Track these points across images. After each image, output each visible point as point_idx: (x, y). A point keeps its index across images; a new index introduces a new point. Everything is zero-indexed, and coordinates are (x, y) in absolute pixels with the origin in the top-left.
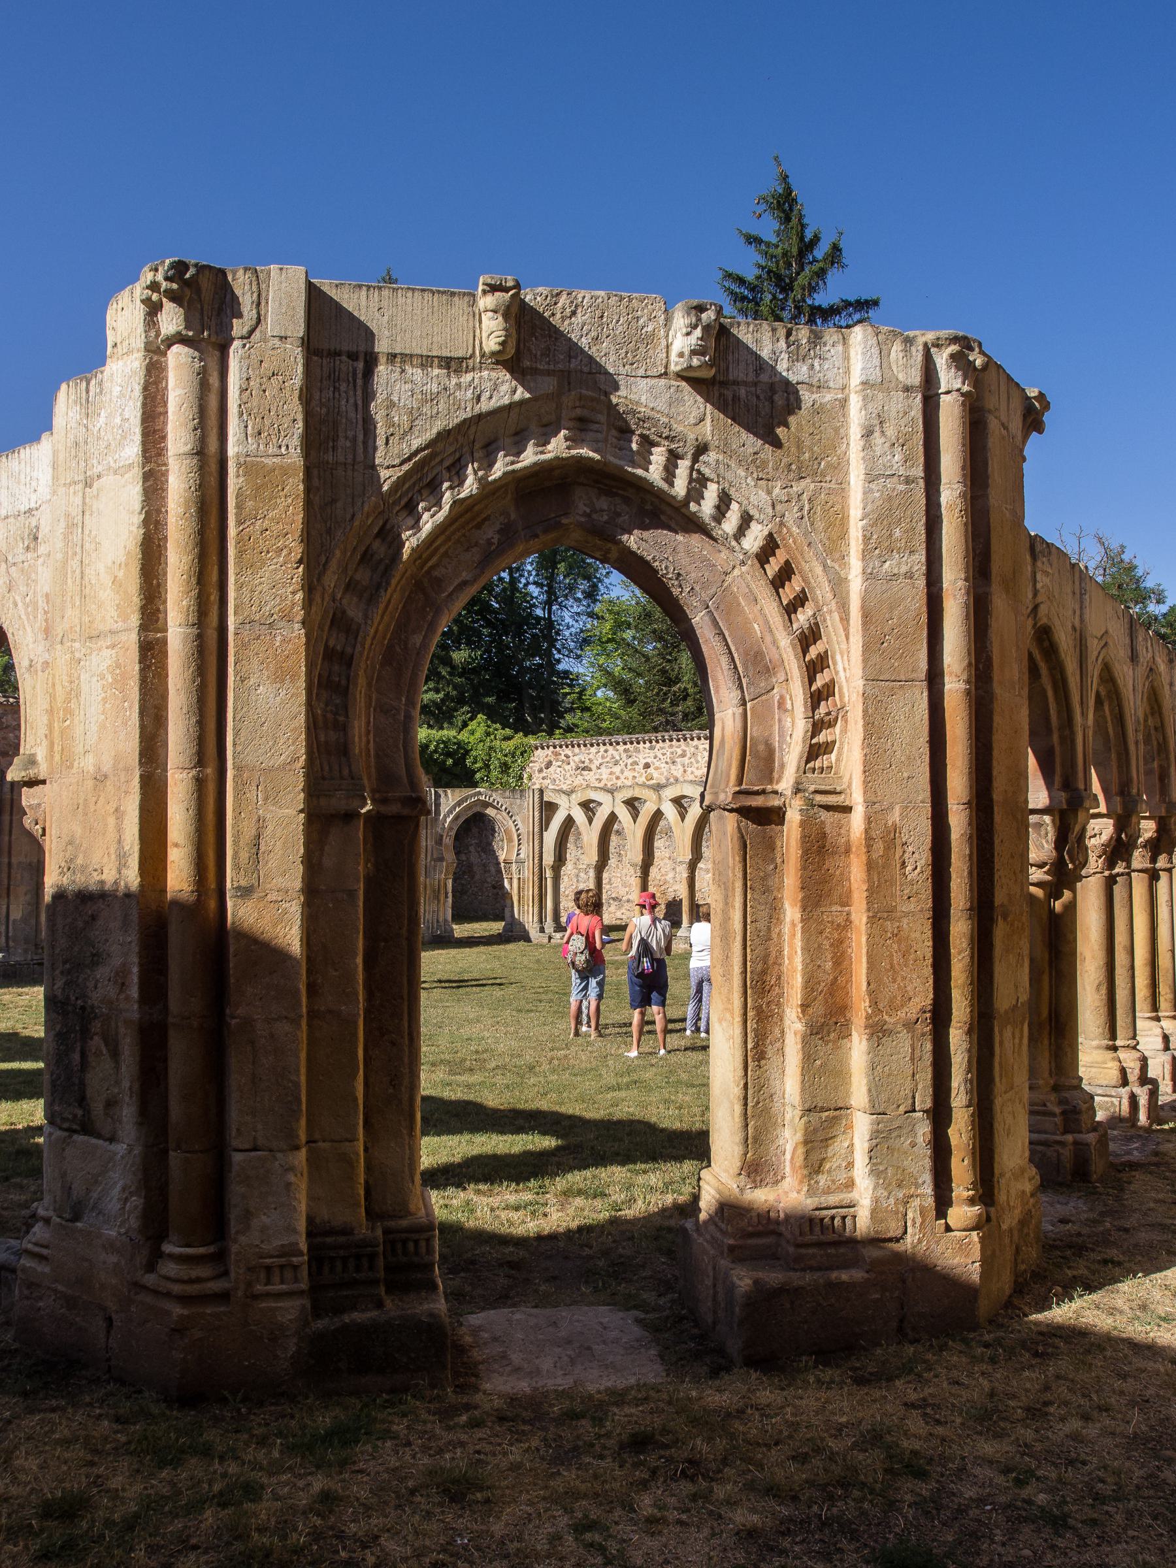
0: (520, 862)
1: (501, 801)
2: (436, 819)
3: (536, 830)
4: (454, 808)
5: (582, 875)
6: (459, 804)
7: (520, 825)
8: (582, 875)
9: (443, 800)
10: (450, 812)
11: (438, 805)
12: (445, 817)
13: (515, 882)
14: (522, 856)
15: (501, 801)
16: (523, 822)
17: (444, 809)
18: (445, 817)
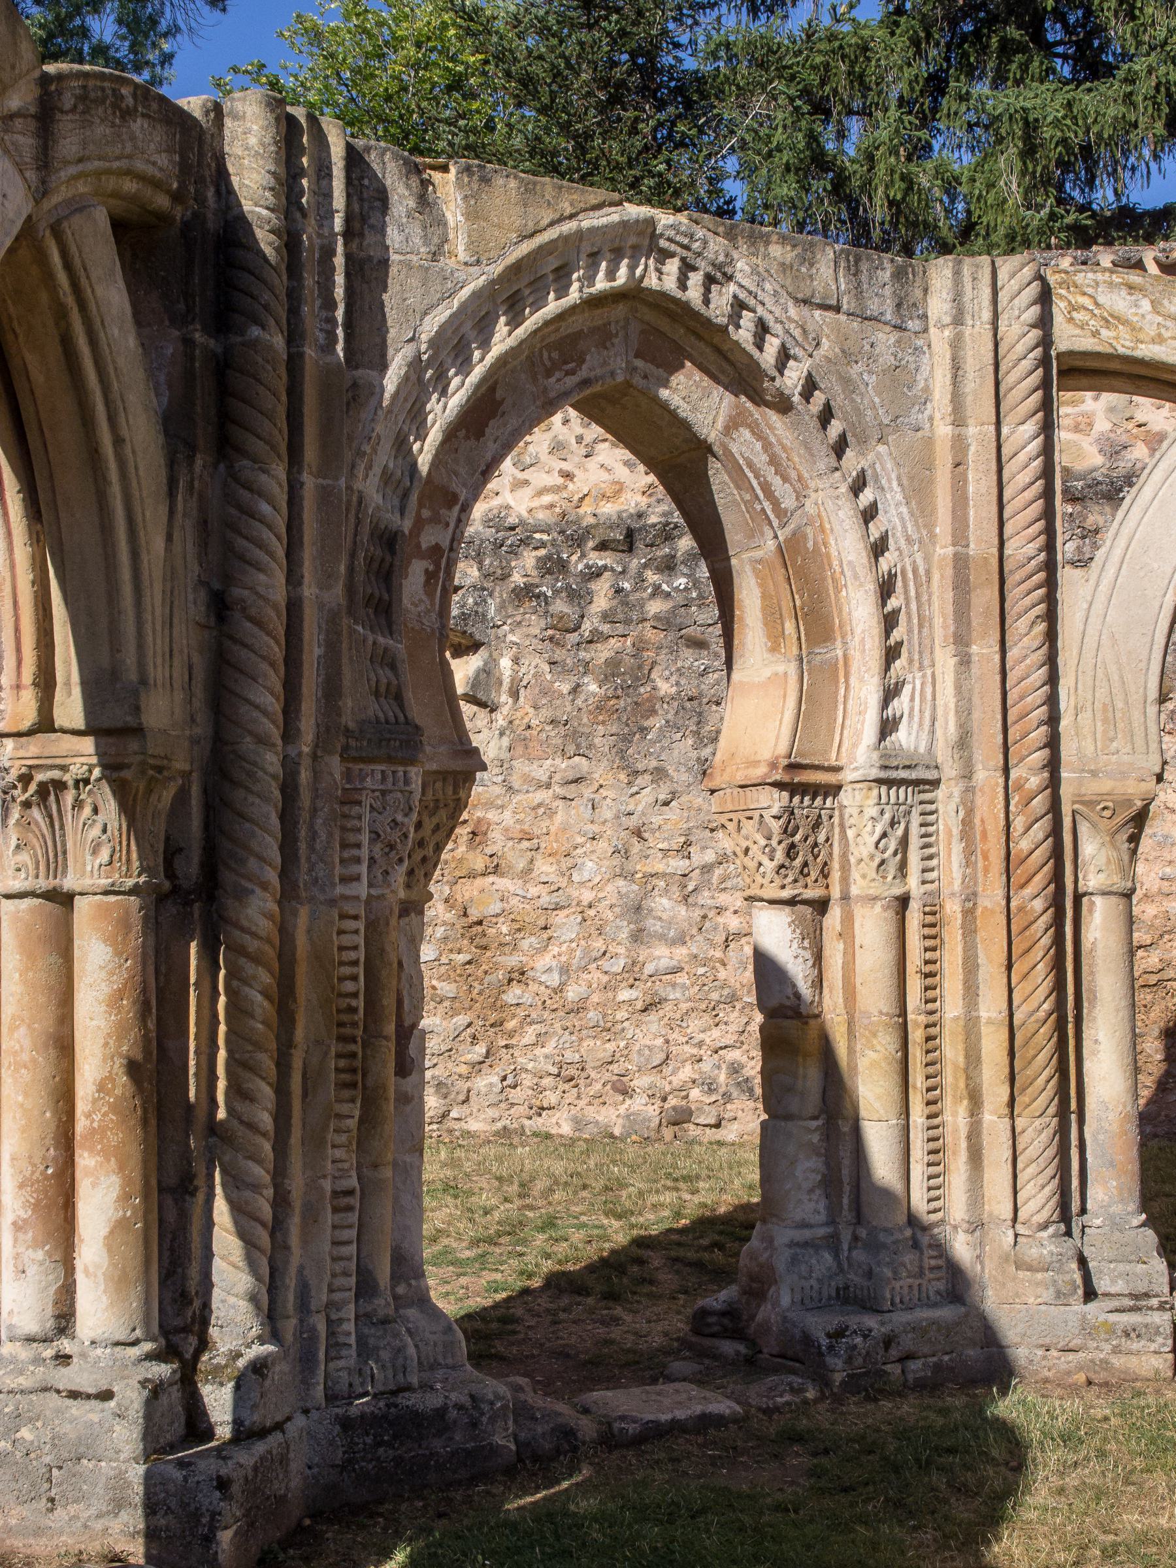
0: (905, 780)
1: (783, 314)
2: (351, 391)
3: (1023, 547)
4: (474, 324)
5: (664, 905)
6: (512, 292)
7: (894, 516)
8: (664, 905)
9: (401, 235)
10: (455, 346)
11: (369, 272)
12: (425, 380)
13: (871, 929)
14: (903, 737)
15: (783, 314)
16: (919, 492)
17: (414, 318)
18: (425, 380)
